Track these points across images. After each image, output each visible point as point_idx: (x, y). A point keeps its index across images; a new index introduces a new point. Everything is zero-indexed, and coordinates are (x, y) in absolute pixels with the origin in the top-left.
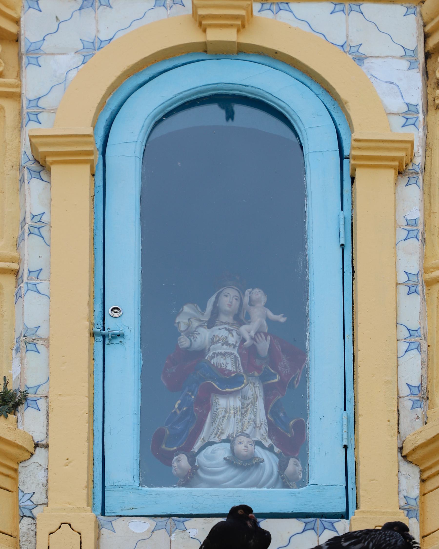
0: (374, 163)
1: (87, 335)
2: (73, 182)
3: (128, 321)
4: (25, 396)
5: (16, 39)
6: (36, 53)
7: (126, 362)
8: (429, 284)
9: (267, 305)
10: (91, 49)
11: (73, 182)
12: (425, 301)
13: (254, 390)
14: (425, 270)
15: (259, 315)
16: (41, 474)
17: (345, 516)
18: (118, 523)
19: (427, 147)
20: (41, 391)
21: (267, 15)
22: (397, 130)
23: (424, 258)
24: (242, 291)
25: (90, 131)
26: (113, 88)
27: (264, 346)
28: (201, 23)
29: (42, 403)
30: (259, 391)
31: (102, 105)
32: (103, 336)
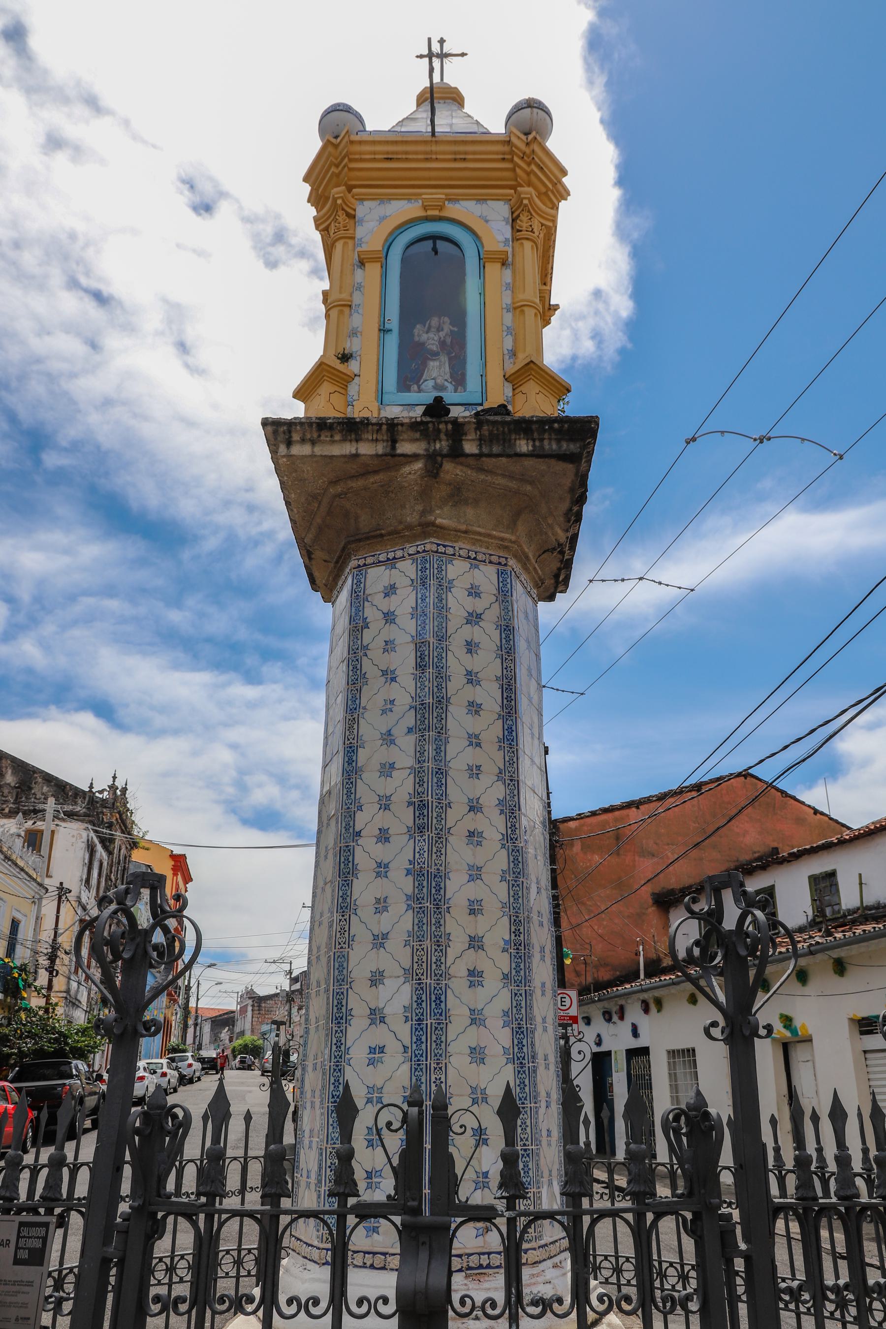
0: (493, 260)
1: (377, 330)
2: (374, 269)
3: (394, 322)
4: (351, 355)
5: (354, 217)
6: (361, 221)
7: (392, 342)
8: (515, 309)
9: (450, 324)
10: (382, 219)
11: (374, 269)
12: (514, 316)
13: (444, 358)
14: (514, 303)
15: (447, 328)
16: (357, 387)
17: (481, 404)
18: (388, 408)
19: (513, 255)
20: (358, 353)
21: (451, 205)
22: (501, 247)
23: (513, 298)
24: (440, 318)
25: (381, 249)
26: (391, 233)
27: (449, 340)
28: (425, 208)
29: (358, 358)
30: (447, 359)
31: (386, 240)
32: (384, 331)
